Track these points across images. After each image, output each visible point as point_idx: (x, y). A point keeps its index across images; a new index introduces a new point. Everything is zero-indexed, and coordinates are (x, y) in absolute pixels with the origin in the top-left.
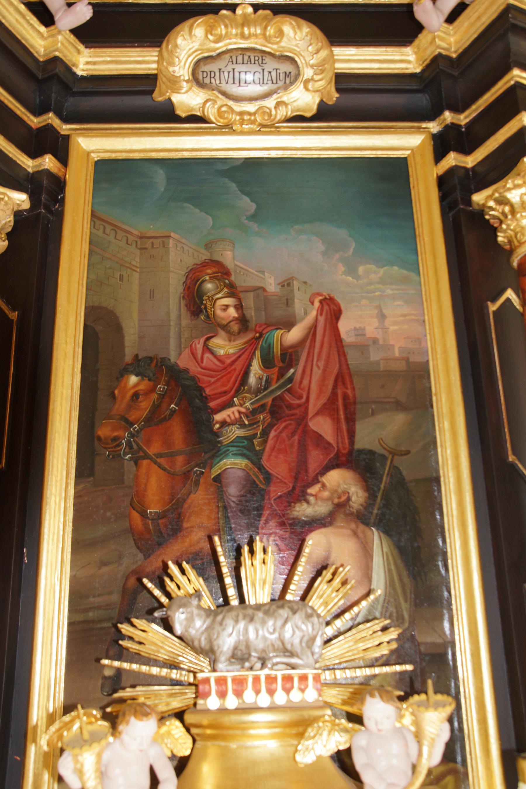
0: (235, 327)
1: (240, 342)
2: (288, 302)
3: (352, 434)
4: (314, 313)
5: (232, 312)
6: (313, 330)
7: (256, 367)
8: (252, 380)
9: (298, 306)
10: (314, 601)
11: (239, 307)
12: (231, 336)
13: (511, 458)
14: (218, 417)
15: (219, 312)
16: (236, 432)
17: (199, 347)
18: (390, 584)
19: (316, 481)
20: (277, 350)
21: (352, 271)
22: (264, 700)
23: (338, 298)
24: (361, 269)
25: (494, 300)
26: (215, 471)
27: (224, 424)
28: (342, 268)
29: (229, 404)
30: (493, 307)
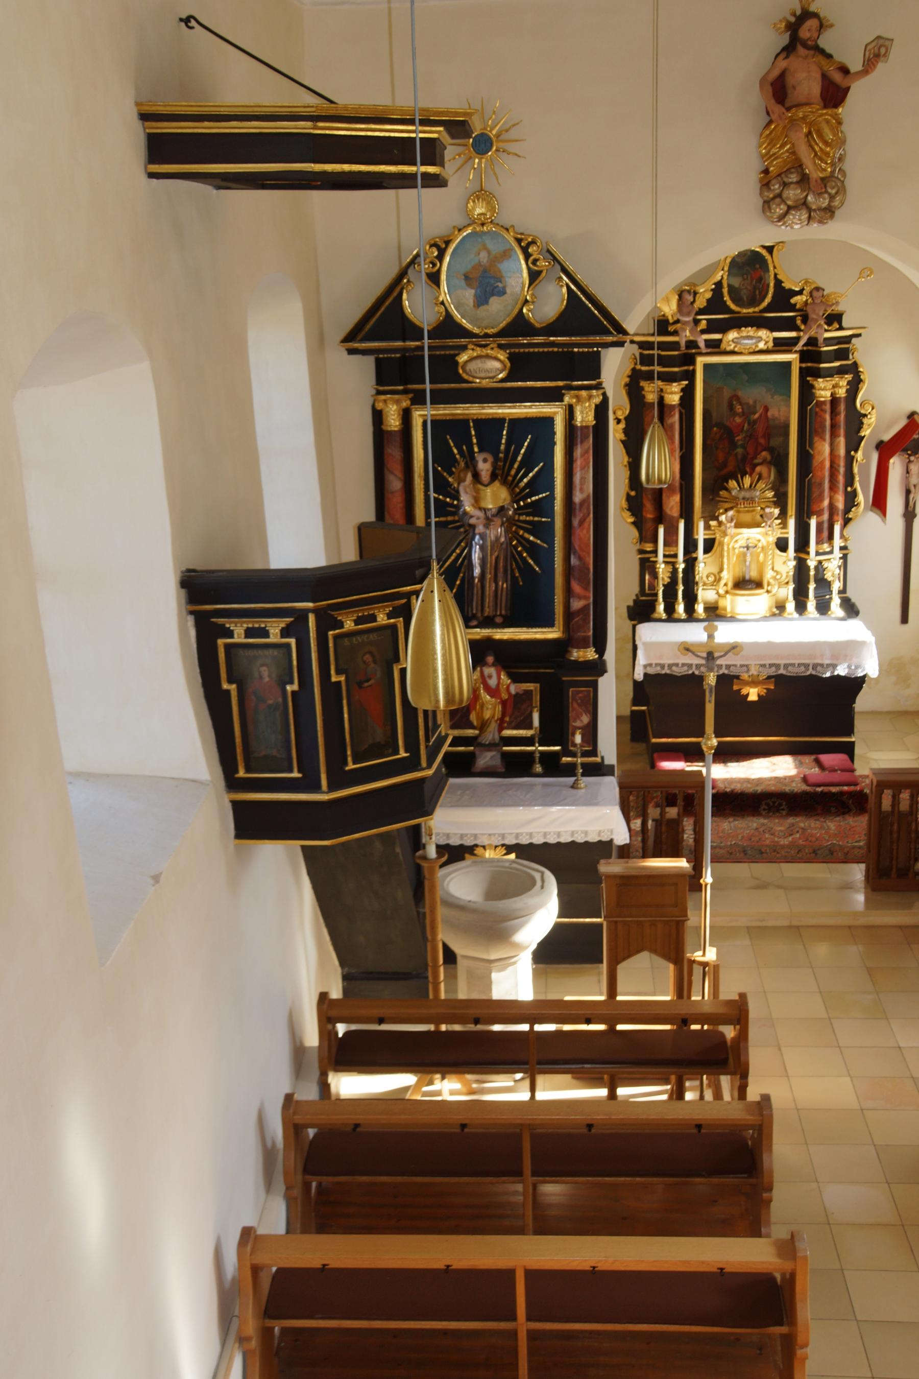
0: (741, 414)
1: (743, 418)
2: (755, 407)
3: (769, 442)
4: (761, 410)
5: (740, 410)
6: (761, 415)
7: (746, 425)
8: (745, 429)
9: (758, 408)
10: (757, 487)
11: (742, 409)
12: (740, 417)
13: (808, 448)
14: (737, 438)
15: (737, 410)
16: (740, 443)
17: (732, 419)
18: (775, 478)
19: (759, 454)
20: (752, 421)
21: (772, 397)
22: (748, 506)
23: (769, 407)
24: (775, 397)
25: (810, 405)
26: (736, 452)
27: (738, 440)
28: (770, 396)
29: (739, 435)
30: (809, 408)
